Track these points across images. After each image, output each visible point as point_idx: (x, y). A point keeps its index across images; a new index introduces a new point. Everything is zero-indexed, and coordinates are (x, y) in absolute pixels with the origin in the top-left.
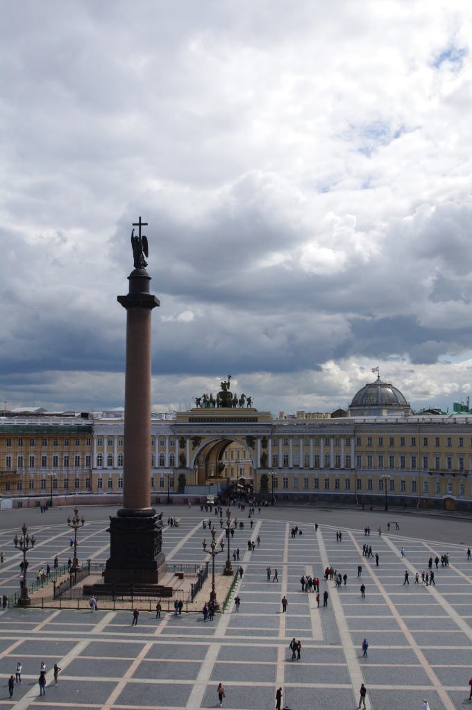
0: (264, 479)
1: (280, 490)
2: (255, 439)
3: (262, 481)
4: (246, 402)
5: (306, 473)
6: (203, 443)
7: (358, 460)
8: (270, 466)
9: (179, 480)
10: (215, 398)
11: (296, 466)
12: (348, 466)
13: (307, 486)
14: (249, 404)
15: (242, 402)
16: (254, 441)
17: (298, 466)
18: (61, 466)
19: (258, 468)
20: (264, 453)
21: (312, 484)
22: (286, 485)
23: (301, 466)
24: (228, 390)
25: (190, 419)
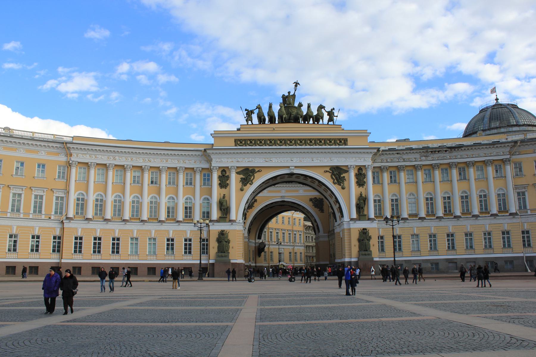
0: (364, 235)
2: (346, 171)
3: (359, 240)
4: (326, 117)
5: (432, 226)
6: (259, 180)
7: (519, 199)
8: (372, 215)
9: (219, 241)
12: (503, 208)
13: (434, 247)
14: (331, 119)
15: (318, 118)
17: (416, 215)
19: (352, 219)
21: (442, 243)
22: (397, 246)
23: (423, 214)
25: (235, 141)
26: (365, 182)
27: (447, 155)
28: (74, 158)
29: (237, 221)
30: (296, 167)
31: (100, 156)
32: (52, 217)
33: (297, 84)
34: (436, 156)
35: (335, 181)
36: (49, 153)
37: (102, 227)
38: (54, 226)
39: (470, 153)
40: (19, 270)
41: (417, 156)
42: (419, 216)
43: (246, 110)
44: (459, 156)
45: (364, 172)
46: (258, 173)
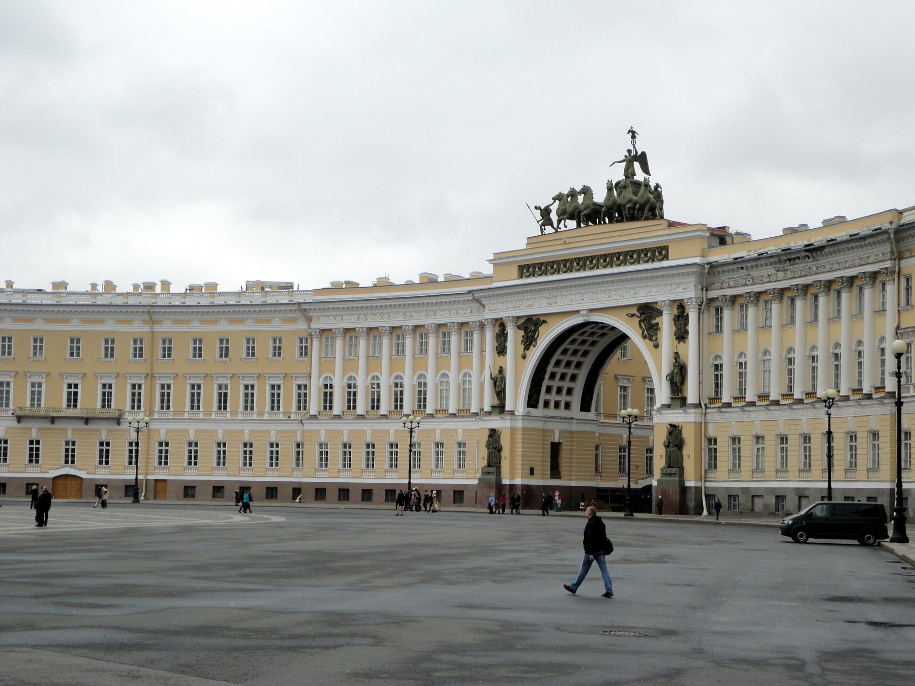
1: (722, 481)
2: (660, 313)
9: (488, 446)
10: (581, 199)
11: (764, 397)
16: (657, 320)
18: (235, 413)
20: (677, 356)
24: (640, 176)
25: (521, 268)
26: (687, 332)
27: (811, 264)
28: (313, 326)
29: (517, 413)
30: (591, 310)
31: (349, 317)
32: (293, 417)
33: (633, 134)
34: (799, 267)
35: (646, 332)
36: (285, 320)
37: (351, 429)
38: (294, 429)
39: (841, 257)
40: (356, 495)
41: (771, 270)
42: (772, 398)
43: (536, 208)
44: (828, 267)
45: (687, 311)
46: (544, 325)
